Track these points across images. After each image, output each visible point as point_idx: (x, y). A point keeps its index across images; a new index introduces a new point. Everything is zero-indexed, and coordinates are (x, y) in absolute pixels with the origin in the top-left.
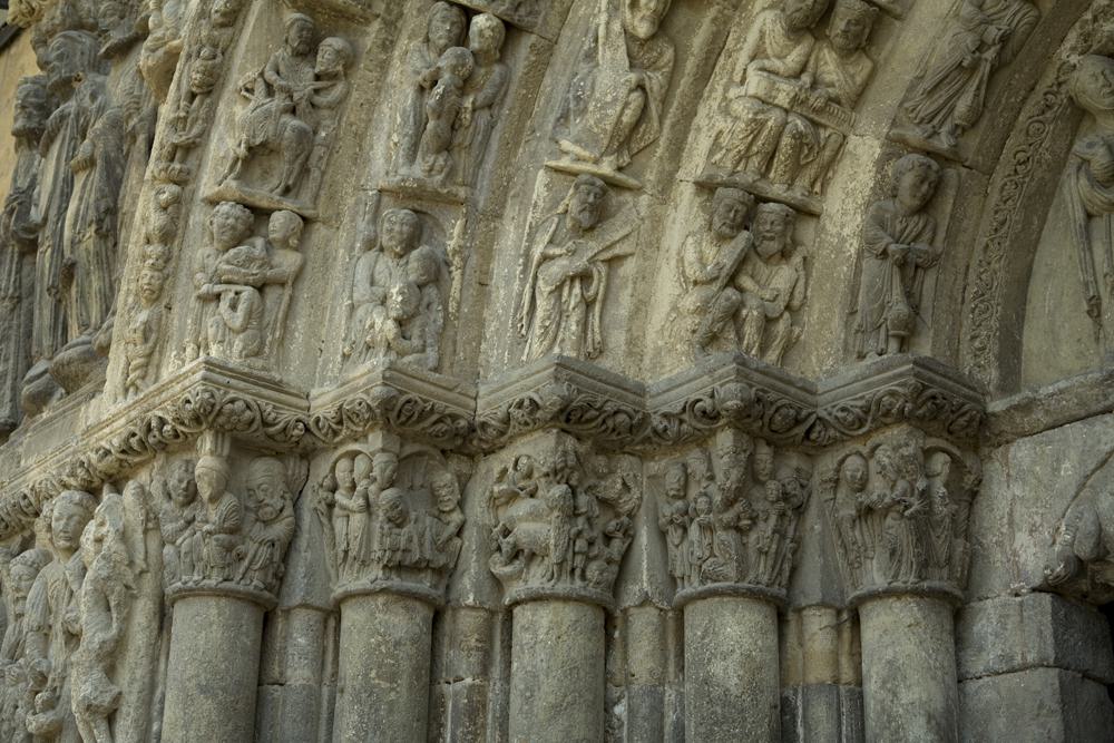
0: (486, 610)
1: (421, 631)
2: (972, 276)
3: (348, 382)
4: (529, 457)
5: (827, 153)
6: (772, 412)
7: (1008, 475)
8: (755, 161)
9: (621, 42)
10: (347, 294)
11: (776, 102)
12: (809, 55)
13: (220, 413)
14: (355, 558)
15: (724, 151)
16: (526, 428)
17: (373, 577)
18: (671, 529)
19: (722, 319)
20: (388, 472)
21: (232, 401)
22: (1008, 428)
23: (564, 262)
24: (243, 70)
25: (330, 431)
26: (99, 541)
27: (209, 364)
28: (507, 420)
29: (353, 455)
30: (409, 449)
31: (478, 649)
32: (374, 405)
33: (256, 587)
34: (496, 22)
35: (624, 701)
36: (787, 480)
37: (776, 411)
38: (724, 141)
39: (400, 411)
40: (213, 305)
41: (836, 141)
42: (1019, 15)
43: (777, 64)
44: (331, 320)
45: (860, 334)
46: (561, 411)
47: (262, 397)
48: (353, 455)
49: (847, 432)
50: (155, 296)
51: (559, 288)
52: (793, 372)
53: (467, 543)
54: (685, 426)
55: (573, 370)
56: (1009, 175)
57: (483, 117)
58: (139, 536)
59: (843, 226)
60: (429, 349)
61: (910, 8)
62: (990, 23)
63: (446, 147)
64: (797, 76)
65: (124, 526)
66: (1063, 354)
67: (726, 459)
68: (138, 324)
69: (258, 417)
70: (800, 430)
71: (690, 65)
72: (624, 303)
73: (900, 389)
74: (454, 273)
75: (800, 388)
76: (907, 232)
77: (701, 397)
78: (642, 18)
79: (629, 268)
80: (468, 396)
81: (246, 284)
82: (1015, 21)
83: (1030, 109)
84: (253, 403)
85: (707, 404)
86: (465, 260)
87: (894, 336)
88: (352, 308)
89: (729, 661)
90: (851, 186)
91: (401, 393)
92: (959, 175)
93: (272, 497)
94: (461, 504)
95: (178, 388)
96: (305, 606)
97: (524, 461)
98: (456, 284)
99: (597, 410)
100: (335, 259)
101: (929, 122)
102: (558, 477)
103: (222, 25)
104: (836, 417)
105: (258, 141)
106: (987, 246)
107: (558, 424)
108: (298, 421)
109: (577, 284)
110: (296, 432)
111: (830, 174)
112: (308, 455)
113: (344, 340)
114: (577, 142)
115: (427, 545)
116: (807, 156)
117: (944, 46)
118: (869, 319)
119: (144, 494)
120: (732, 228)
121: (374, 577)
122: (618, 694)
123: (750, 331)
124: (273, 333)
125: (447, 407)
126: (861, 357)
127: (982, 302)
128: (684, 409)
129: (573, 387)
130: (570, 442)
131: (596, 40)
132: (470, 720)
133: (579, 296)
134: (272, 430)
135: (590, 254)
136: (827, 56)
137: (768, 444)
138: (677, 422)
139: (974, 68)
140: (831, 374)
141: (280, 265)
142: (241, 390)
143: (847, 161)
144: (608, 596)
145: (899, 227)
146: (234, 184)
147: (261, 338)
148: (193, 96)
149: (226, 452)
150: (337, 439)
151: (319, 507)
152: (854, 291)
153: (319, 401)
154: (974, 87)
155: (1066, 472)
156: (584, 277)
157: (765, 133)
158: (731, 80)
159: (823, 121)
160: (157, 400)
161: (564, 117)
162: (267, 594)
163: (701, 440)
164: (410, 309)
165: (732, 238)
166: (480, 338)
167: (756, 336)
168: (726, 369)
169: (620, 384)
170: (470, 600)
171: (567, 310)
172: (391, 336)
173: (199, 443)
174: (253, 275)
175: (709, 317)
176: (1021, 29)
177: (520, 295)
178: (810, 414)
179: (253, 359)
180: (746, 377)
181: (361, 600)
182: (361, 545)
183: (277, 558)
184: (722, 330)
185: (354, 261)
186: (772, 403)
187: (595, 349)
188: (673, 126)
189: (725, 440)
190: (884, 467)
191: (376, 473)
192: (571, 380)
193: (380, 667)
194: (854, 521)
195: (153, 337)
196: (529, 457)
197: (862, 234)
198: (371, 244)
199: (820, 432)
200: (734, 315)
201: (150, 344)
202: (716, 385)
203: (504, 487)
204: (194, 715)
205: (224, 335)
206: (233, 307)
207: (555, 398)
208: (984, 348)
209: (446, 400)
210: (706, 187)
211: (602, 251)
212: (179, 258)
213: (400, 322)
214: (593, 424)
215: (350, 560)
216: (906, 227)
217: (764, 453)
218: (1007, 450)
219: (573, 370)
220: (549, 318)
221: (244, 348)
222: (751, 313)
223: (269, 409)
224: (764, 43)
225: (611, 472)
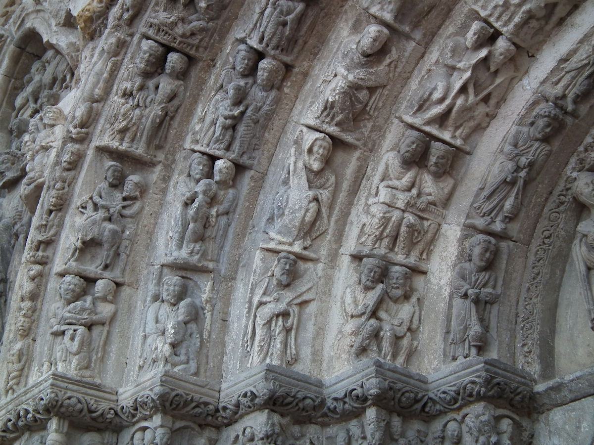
2: (521, 308)
5: (429, 235)
6: (399, 396)
7: (550, 431)
8: (386, 242)
9: (303, 173)
10: (141, 329)
11: (397, 206)
12: (416, 177)
13: (62, 406)
15: (367, 235)
16: (250, 410)
19: (368, 338)
20: (165, 440)
21: (69, 398)
22: (546, 401)
23: (272, 305)
24: (80, 195)
25: (130, 415)
27: (55, 376)
28: (238, 405)
29: (144, 429)
30: (179, 424)
32: (155, 398)
34: (229, 163)
36: (412, 438)
37: (403, 394)
38: (367, 229)
39: (172, 402)
40: (60, 338)
41: (434, 228)
42: (539, 151)
43: (396, 183)
44: (132, 345)
45: (453, 345)
46: (270, 398)
48: (144, 429)
49: (447, 407)
50: (25, 333)
51: (269, 322)
52: (413, 369)
54: (347, 406)
55: (276, 373)
56: (540, 245)
57: (223, 220)
59: (440, 279)
60: (191, 362)
61: (475, 147)
62: (522, 155)
63: (200, 238)
64: (409, 190)
66: (579, 354)
67: (372, 426)
68: (15, 351)
69: (86, 408)
70: (419, 406)
71: (345, 186)
72: (310, 329)
73: (477, 380)
74: (206, 315)
75: (416, 380)
76: (479, 282)
77: (355, 387)
78: (315, 160)
79: (312, 308)
80: (215, 390)
81: (81, 325)
82: (537, 154)
83: (550, 205)
84: (82, 398)
85: (359, 391)
86: (213, 306)
87: (473, 346)
88: (145, 337)
90: (444, 254)
91: (173, 390)
92: (509, 246)
95: (36, 390)
97: (248, 430)
98: (208, 321)
99: (292, 397)
100: (135, 307)
101: (488, 216)
102: (269, 440)
103: (68, 170)
104: (440, 397)
105: (88, 238)
106: (529, 288)
107: (268, 406)
108: (111, 409)
109: (280, 319)
110: (109, 416)
111: (432, 247)
113: (140, 357)
114: (279, 233)
116: (417, 238)
117: (496, 169)
118: (458, 336)
120: (373, 282)
123: (386, 345)
124: (97, 354)
125: (201, 398)
126: (454, 359)
127: (528, 323)
128: (346, 395)
129: (277, 383)
130: (276, 418)
131: (289, 173)
133: (282, 326)
134: (94, 415)
135: (288, 300)
136: (426, 178)
137: (399, 415)
138: (342, 404)
139: (513, 183)
140: (436, 370)
141: (101, 313)
142: (76, 391)
143: (441, 240)
145: (473, 279)
146: (74, 264)
147: (89, 358)
148: (51, 212)
149: (65, 429)
150: (135, 420)
152: (449, 320)
153: (124, 396)
154: (514, 194)
155: (584, 428)
156: (285, 315)
157: (391, 224)
158: (370, 194)
159: (425, 216)
160: (24, 398)
161: (271, 220)
163: (358, 414)
164: (179, 337)
165: (373, 288)
166: (223, 353)
167: (389, 348)
168: (369, 369)
169: (305, 380)
171: (275, 335)
172: (167, 354)
173: (49, 425)
174: (84, 319)
175: (360, 337)
176: (541, 158)
177: (246, 327)
178: (424, 396)
179: (85, 371)
180: (382, 374)
184: (369, 345)
185: (146, 309)
186: (399, 390)
187: (292, 359)
188: (336, 222)
189: (371, 413)
190: (470, 429)
192: (275, 379)
195: (24, 358)
196: (252, 428)
197: (451, 284)
198: (156, 298)
199: (431, 407)
200: (376, 335)
201: (22, 363)
202: (364, 380)
205: (66, 357)
206: (72, 339)
207: (265, 391)
208: (530, 352)
210: (357, 258)
211: (294, 298)
212: (41, 309)
213: (174, 346)
214: (291, 406)
216: (479, 278)
217: (396, 422)
218: (548, 415)
219: (276, 373)
220: (263, 340)
221: (78, 364)
222: (386, 334)
223: (92, 402)
224: (388, 171)
225: (303, 436)
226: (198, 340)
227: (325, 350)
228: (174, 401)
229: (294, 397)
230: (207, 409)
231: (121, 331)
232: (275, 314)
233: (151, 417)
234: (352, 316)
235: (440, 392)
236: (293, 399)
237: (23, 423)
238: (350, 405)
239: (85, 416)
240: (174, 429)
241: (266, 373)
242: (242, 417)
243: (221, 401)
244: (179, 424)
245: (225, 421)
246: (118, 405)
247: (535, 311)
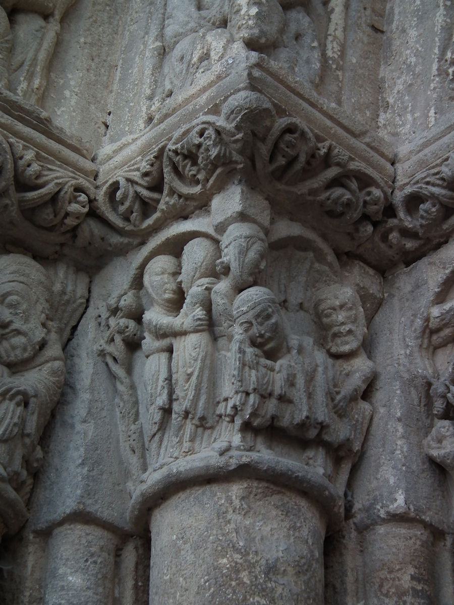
1: (312, 552)
3: (175, 110)
10: (154, 31)
17: (221, 444)
20: (252, 255)
25: (136, 207)
29: (175, 247)
30: (286, 229)
31: (416, 593)
39: (276, 146)
47: (16, 134)
53: (382, 410)
88: (163, 53)
93: (27, 321)
94: (368, 346)
96: (81, 517)
108: (78, 189)
110: (74, 207)
113: (150, 98)
115: (320, 396)
121: (224, 445)
124: (30, 77)
150: (150, 221)
151: (110, 349)
170: (399, 502)
181: (198, 491)
182: (198, 389)
183: (32, 425)
191: (230, 255)
209: (350, 148)
215: (175, 418)
223: (29, 155)
226: (316, 54)
228: (282, 146)
230: (362, 196)
231: (92, 45)
233: (202, 205)
240: (274, 237)
243: (398, 184)
244: (286, 229)
245: (410, 245)
246: (97, 187)
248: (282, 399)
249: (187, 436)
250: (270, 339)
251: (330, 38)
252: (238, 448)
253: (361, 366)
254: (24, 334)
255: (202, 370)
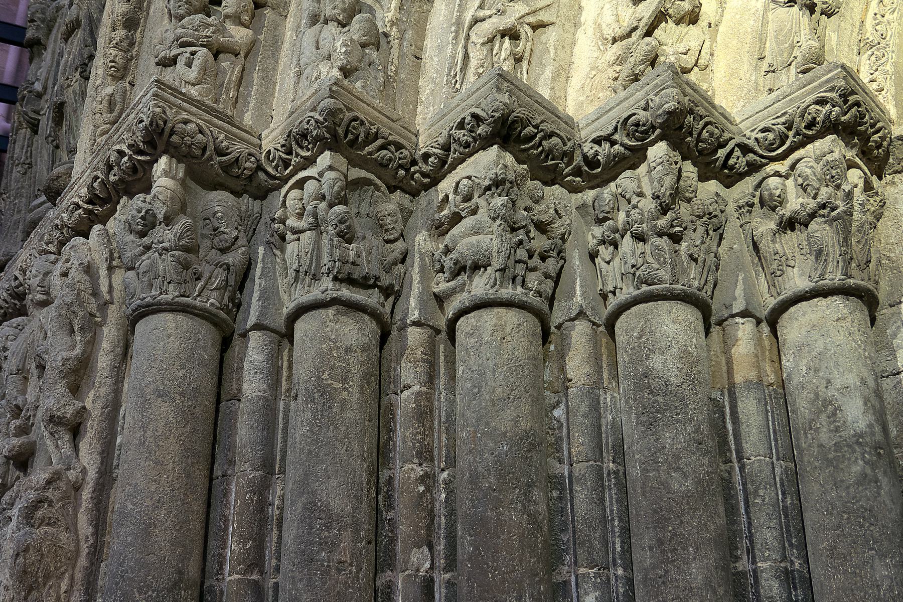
0: (432, 327)
4: (469, 178)
14: (306, 272)
17: (323, 288)
18: (602, 248)
23: (494, 20)
25: (281, 163)
26: (65, 275)
28: (446, 148)
31: (423, 360)
33: (212, 304)
35: (562, 406)
50: (119, 74)
51: (491, 40)
55: (513, 84)
58: (103, 272)
65: (89, 262)
75: (720, 113)
79: (551, 36)
80: (410, 131)
81: (202, 46)
86: (402, 33)
88: (300, 74)
89: (667, 355)
91: (350, 110)
96: (258, 327)
99: (534, 127)
104: (756, 139)
110: (248, 164)
112: (262, 194)
119: (108, 238)
122: (557, 399)
124: (228, 90)
125: (390, 134)
132: (419, 422)
133: (509, 49)
135: (518, 15)
138: (608, 145)
144: (545, 307)
150: (288, 171)
151: (272, 240)
156: (513, 34)
162: (223, 315)
173: (154, 169)
178: (731, 139)
185: (300, 36)
186: (701, 118)
190: (806, 179)
193: (332, 369)
194: (774, 234)
196: (469, 178)
198: (314, 19)
201: (115, 113)
203: (446, 212)
204: (152, 416)
211: (528, 14)
212: (141, 43)
217: (690, 170)
227: (569, 98)
229: (536, 127)
232: (499, 31)
234: (614, 40)
235: (757, 130)
236: (536, 131)
237: (116, 178)
238: (622, 145)
239: (210, 159)
241: (497, 80)
242: (453, 167)
247: (890, 33)
248: (353, 264)
249: (306, 285)
250: (347, 233)
251: (390, 64)
252: (331, 290)
253: (400, 245)
254: (226, 234)
255: (313, 250)
